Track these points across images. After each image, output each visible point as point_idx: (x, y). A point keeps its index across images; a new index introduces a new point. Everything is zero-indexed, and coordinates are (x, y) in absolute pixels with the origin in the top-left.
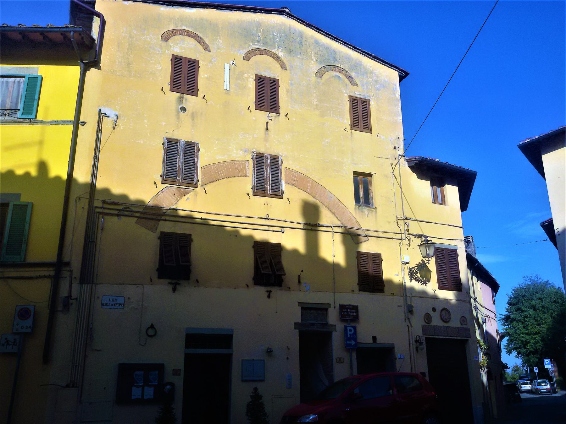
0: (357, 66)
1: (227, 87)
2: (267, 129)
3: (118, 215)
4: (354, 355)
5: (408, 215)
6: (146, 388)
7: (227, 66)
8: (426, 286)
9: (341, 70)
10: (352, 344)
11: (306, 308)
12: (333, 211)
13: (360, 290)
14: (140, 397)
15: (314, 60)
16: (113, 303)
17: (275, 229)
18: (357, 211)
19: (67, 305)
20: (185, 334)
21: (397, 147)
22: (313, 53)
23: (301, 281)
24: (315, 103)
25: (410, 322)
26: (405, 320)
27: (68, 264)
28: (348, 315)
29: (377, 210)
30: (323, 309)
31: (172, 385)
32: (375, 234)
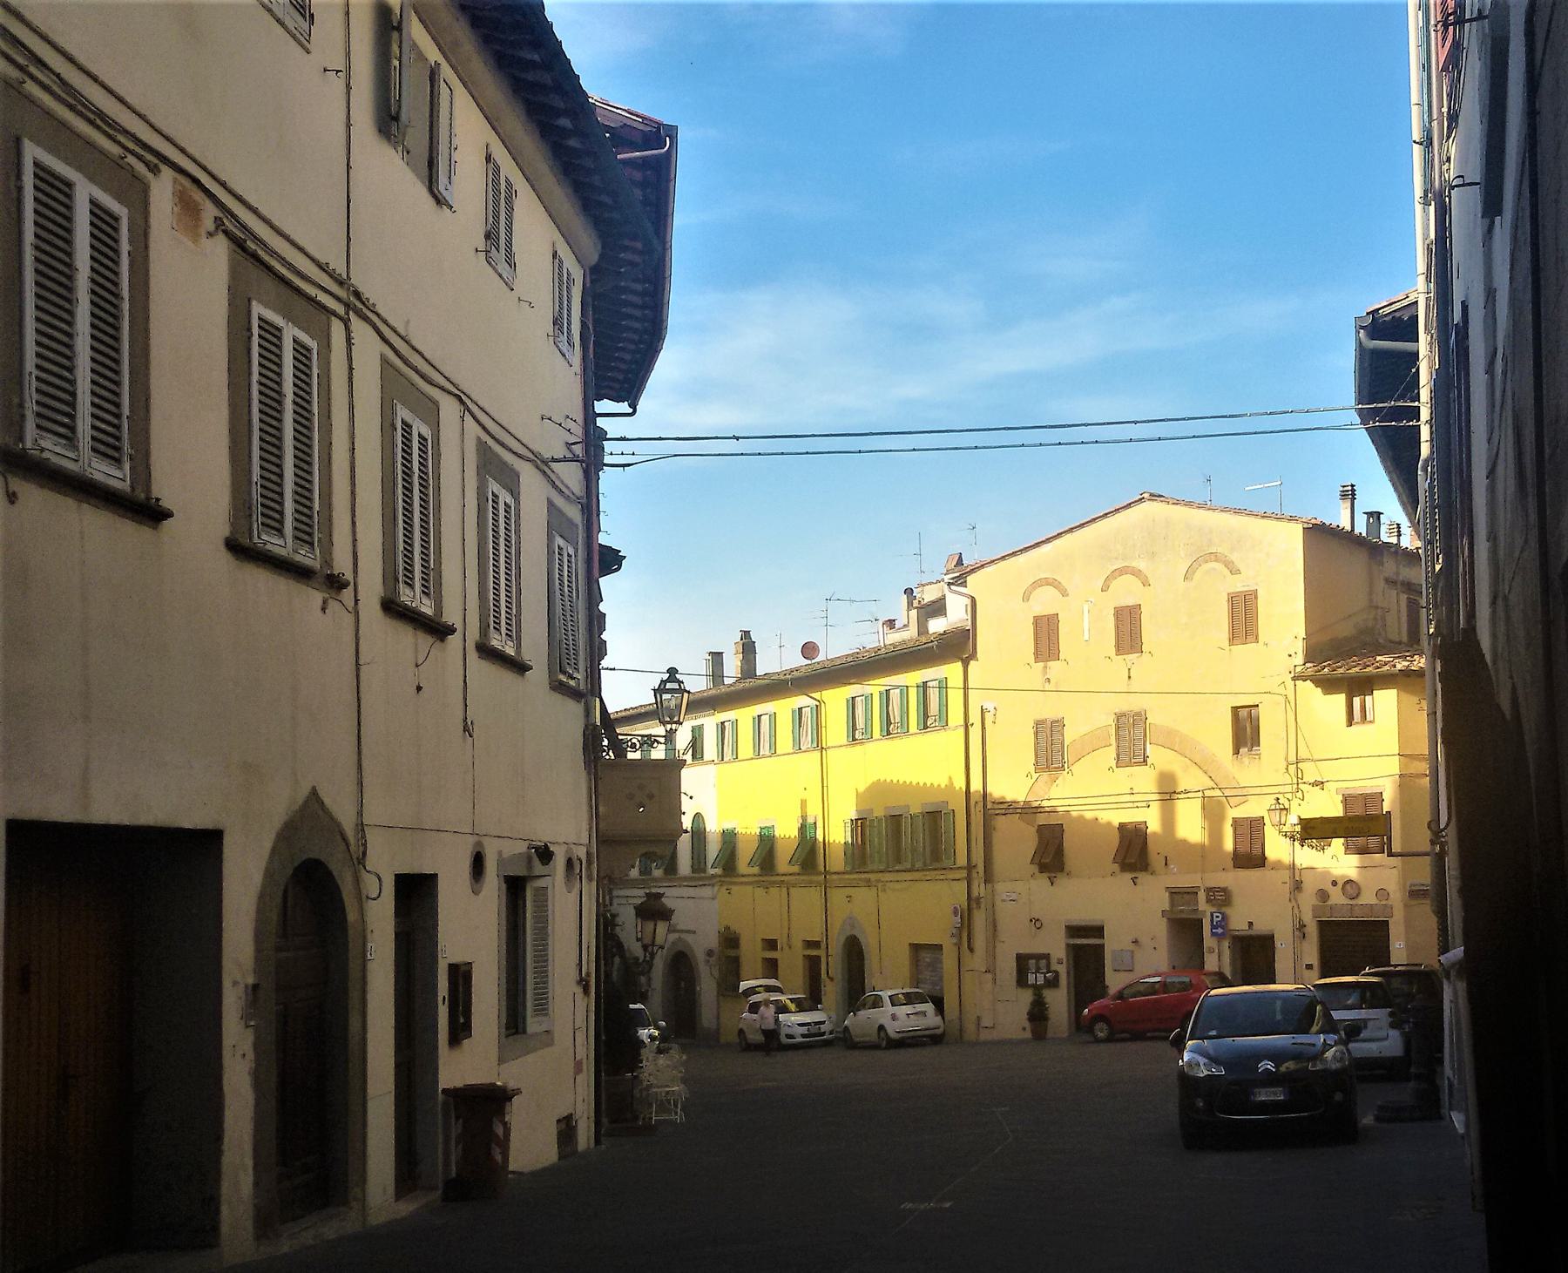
2: (1129, 677)
4: (1226, 944)
5: (1303, 754)
9: (1215, 557)
11: (1174, 893)
17: (1139, 804)
22: (1182, 545)
26: (1290, 900)
30: (1192, 893)
31: (1056, 972)
32: (1258, 791)
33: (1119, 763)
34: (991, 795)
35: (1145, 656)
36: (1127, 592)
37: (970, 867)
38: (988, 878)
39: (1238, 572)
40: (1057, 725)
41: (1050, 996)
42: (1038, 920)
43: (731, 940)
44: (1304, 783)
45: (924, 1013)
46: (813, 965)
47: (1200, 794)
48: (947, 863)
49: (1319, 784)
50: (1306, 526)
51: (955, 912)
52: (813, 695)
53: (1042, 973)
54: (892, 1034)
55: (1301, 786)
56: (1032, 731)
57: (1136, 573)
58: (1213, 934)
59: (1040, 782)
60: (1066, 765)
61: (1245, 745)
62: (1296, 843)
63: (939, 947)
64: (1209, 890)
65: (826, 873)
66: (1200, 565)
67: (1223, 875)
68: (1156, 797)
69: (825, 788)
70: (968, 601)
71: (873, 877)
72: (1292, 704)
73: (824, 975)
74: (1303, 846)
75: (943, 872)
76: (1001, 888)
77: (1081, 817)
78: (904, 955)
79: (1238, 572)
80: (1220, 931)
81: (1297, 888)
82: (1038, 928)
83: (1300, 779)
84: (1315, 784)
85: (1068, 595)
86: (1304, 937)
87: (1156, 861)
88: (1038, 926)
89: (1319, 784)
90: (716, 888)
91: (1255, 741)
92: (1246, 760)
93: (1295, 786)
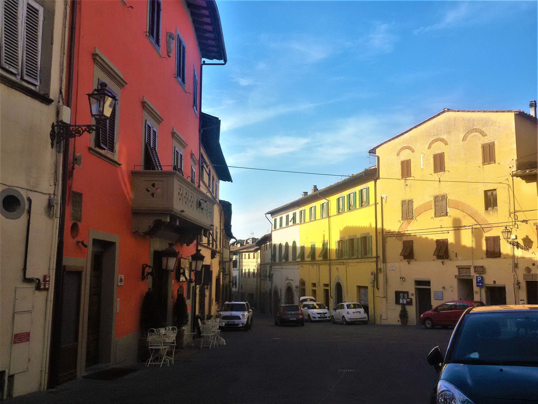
0: (486, 123)
1: (422, 167)
4: (483, 290)
6: (404, 300)
7: (422, 156)
8: (528, 251)
9: (476, 130)
11: (460, 268)
12: (473, 217)
13: (487, 257)
14: (402, 303)
15: (462, 131)
16: (392, 269)
17: (444, 232)
18: (486, 214)
19: (380, 271)
21: (511, 166)
22: (461, 127)
23: (457, 256)
24: (462, 157)
25: (516, 273)
26: (513, 272)
27: (379, 257)
28: (478, 271)
29: (498, 210)
30: (468, 268)
32: (496, 225)
33: (436, 215)
34: (385, 229)
35: (446, 172)
36: (439, 147)
37: (377, 257)
38: (384, 261)
39: (486, 135)
40: (411, 202)
41: (408, 308)
43: (303, 283)
44: (518, 221)
45: (360, 312)
46: (326, 292)
47: (471, 227)
48: (369, 256)
49: (525, 221)
50: (515, 113)
51: (372, 274)
52: (327, 199)
53: (405, 299)
54: (347, 319)
55: (516, 222)
56: (400, 205)
57: (442, 140)
58: (477, 286)
59: (404, 225)
60: (414, 217)
61: (491, 206)
62: (515, 247)
63: (367, 287)
64: (475, 267)
65: (330, 260)
66: (469, 134)
67: (482, 260)
68: (452, 229)
69: (330, 231)
70: (377, 158)
71: (344, 261)
72: (512, 188)
73: (330, 297)
74: (518, 248)
75: (368, 259)
76: (389, 265)
77: (421, 237)
78: (355, 290)
79: (486, 135)
80: (481, 284)
81: (516, 267)
83: (516, 219)
84: (523, 221)
85: (414, 152)
86: (520, 288)
87: (451, 254)
89: (525, 221)
90: (299, 265)
91: (495, 204)
92: (491, 213)
93: (514, 222)
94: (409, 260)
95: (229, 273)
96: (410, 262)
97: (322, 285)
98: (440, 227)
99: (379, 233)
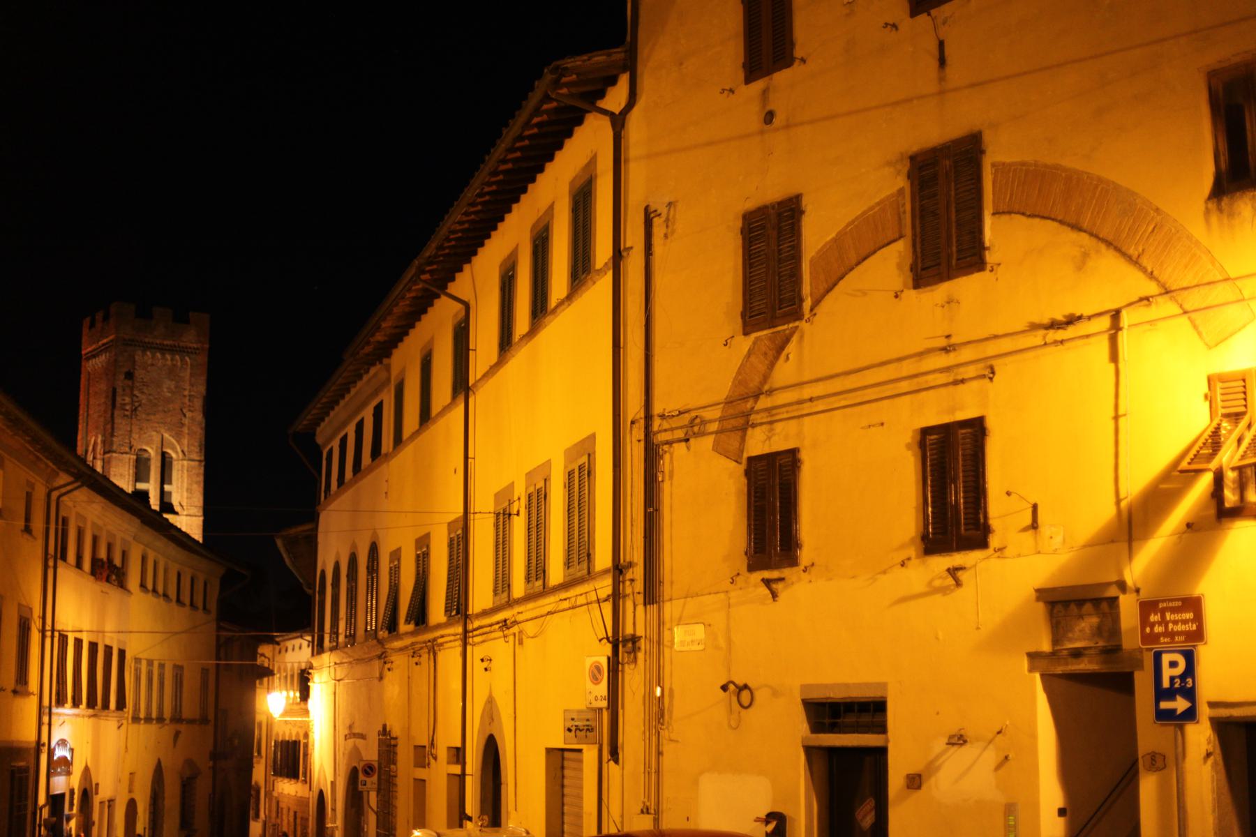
3: (687, 440)
10: (1179, 712)
18: (1214, 219)
20: (799, 701)
38: (651, 595)
42: (746, 687)
80: (1181, 704)
82: (750, 705)
88: (746, 703)
94: (774, 574)
95: (211, 716)
96: (778, 587)
97: (442, 753)
98: (943, 342)
99: (633, 423)
